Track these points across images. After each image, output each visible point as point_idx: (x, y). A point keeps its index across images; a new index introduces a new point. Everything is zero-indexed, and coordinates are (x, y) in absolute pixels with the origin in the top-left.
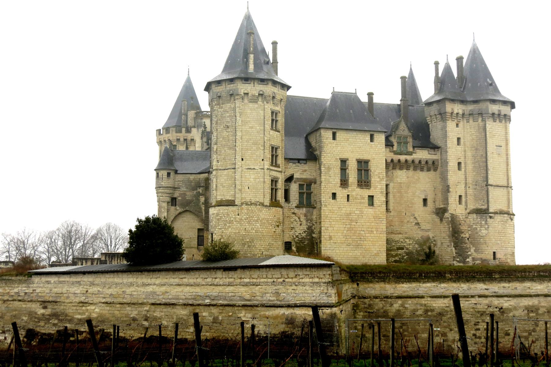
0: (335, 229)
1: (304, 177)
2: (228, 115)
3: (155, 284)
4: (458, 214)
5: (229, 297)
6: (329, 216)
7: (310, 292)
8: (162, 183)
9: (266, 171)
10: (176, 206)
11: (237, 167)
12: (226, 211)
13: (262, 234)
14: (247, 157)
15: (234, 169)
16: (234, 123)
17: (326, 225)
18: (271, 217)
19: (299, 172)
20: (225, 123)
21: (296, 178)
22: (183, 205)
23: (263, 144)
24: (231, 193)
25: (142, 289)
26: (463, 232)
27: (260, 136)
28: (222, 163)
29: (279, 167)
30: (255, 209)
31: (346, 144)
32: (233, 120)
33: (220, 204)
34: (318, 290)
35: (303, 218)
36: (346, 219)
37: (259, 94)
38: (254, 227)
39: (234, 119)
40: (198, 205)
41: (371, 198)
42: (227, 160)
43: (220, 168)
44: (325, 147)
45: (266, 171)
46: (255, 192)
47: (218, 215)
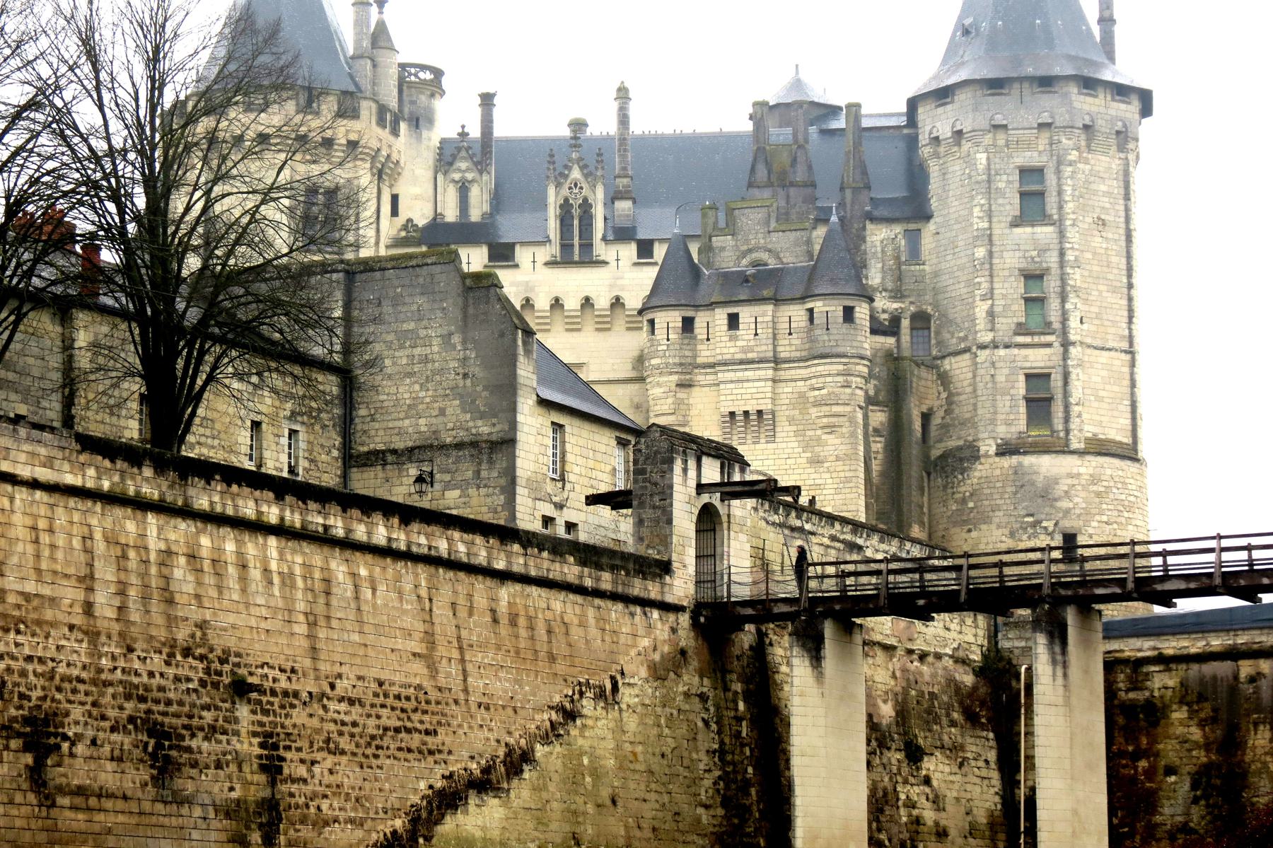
2: (1103, 188)
11: (1137, 347)
12: (1120, 473)
16: (1122, 220)
20: (1098, 210)
28: (1093, 328)
32: (1117, 207)
33: (1100, 448)
39: (1122, 208)
42: (1106, 323)
43: (1089, 341)
47: (1095, 480)
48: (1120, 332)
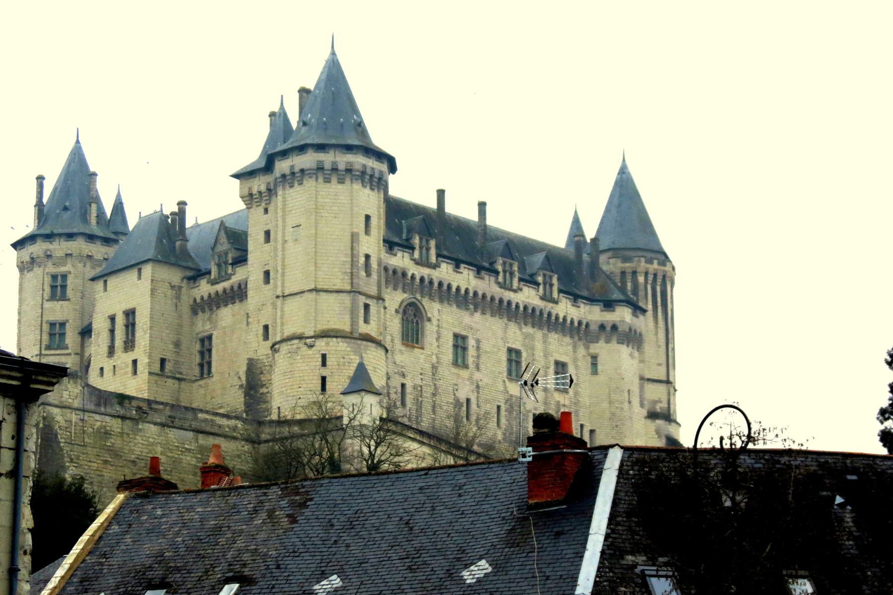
4: (261, 358)
26: (265, 385)
29: (67, 348)
41: (135, 362)
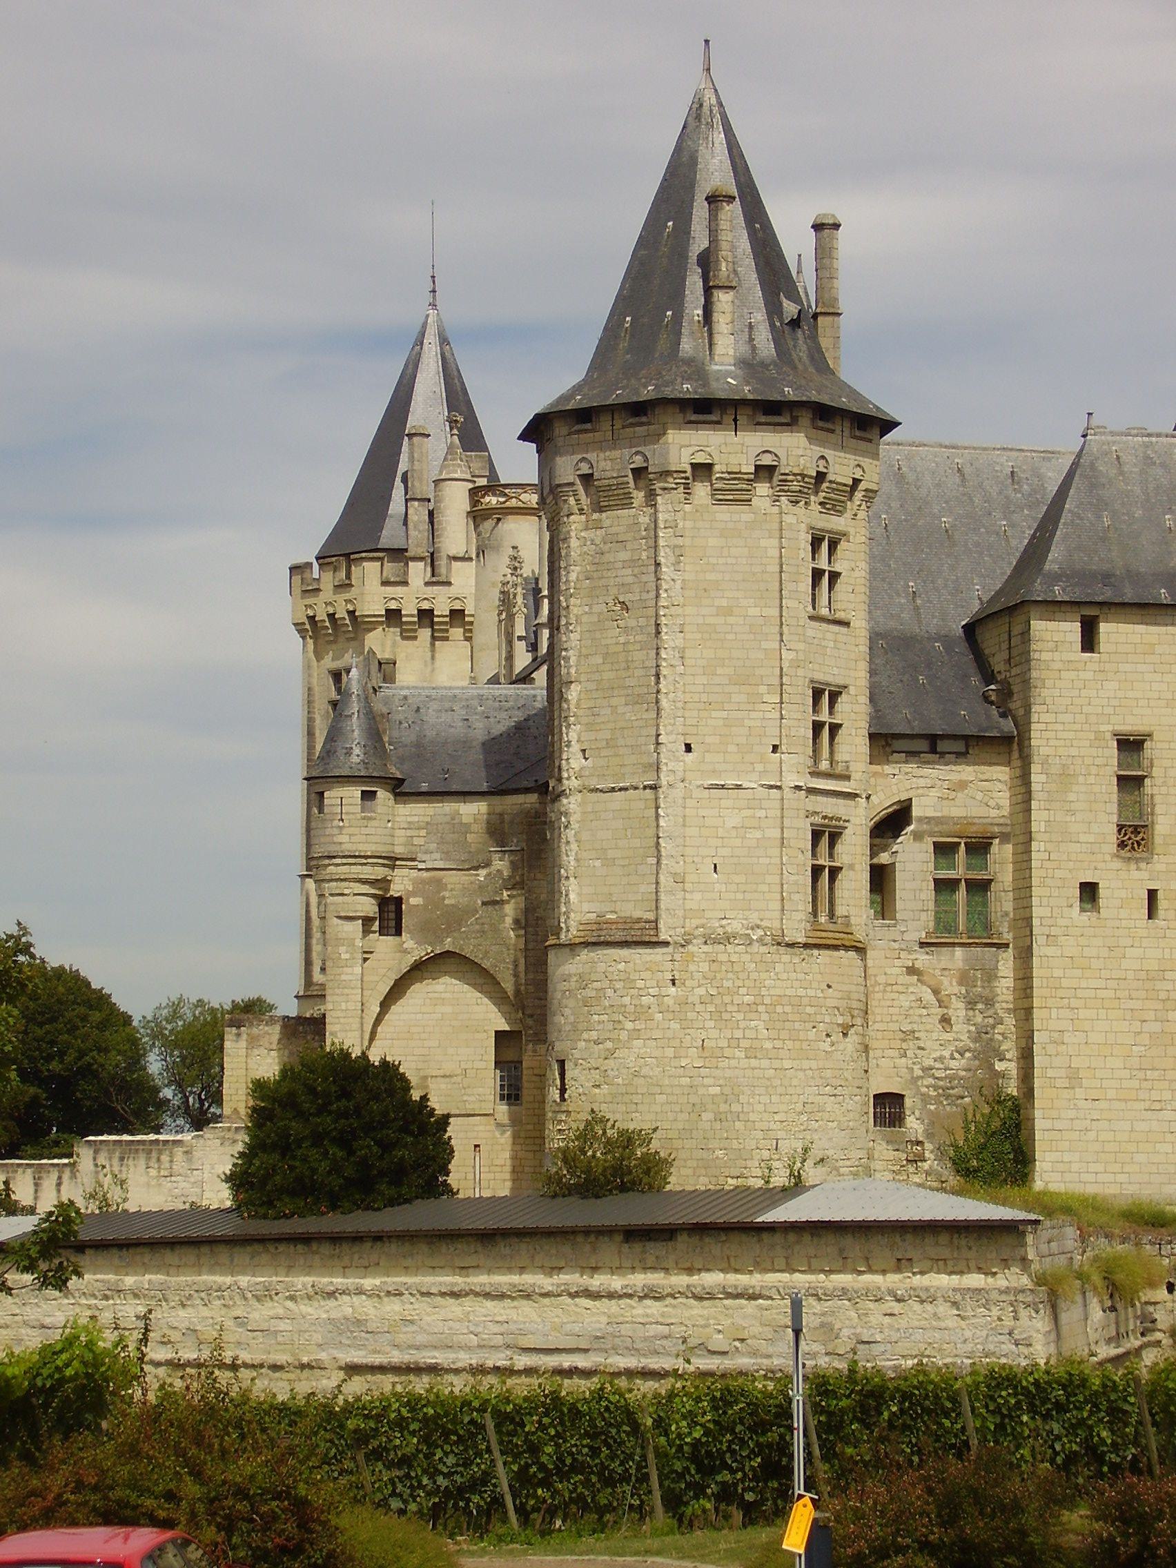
0: (1093, 1038)
1: (956, 812)
2: (624, 555)
3: (360, 1292)
5: (646, 1339)
6: (1065, 983)
7: (950, 1323)
8: (335, 839)
9: (788, 793)
10: (398, 932)
12: (622, 966)
13: (777, 1064)
14: (708, 740)
15: (654, 788)
17: (1053, 1025)
18: (811, 993)
19: (934, 793)
21: (920, 819)
22: (428, 931)
23: (776, 681)
24: (643, 888)
25: (310, 1310)
27: (764, 645)
28: (602, 762)
30: (747, 958)
31: (1141, 668)
34: (983, 1317)
35: (951, 987)
36: (1143, 994)
37: (758, 468)
38: (738, 1034)
40: (496, 930)
42: (622, 751)
43: (593, 783)
44: (1048, 683)
45: (788, 793)
46: (742, 888)
48: (645, 759)
